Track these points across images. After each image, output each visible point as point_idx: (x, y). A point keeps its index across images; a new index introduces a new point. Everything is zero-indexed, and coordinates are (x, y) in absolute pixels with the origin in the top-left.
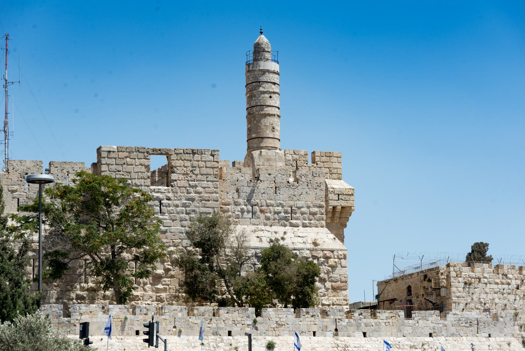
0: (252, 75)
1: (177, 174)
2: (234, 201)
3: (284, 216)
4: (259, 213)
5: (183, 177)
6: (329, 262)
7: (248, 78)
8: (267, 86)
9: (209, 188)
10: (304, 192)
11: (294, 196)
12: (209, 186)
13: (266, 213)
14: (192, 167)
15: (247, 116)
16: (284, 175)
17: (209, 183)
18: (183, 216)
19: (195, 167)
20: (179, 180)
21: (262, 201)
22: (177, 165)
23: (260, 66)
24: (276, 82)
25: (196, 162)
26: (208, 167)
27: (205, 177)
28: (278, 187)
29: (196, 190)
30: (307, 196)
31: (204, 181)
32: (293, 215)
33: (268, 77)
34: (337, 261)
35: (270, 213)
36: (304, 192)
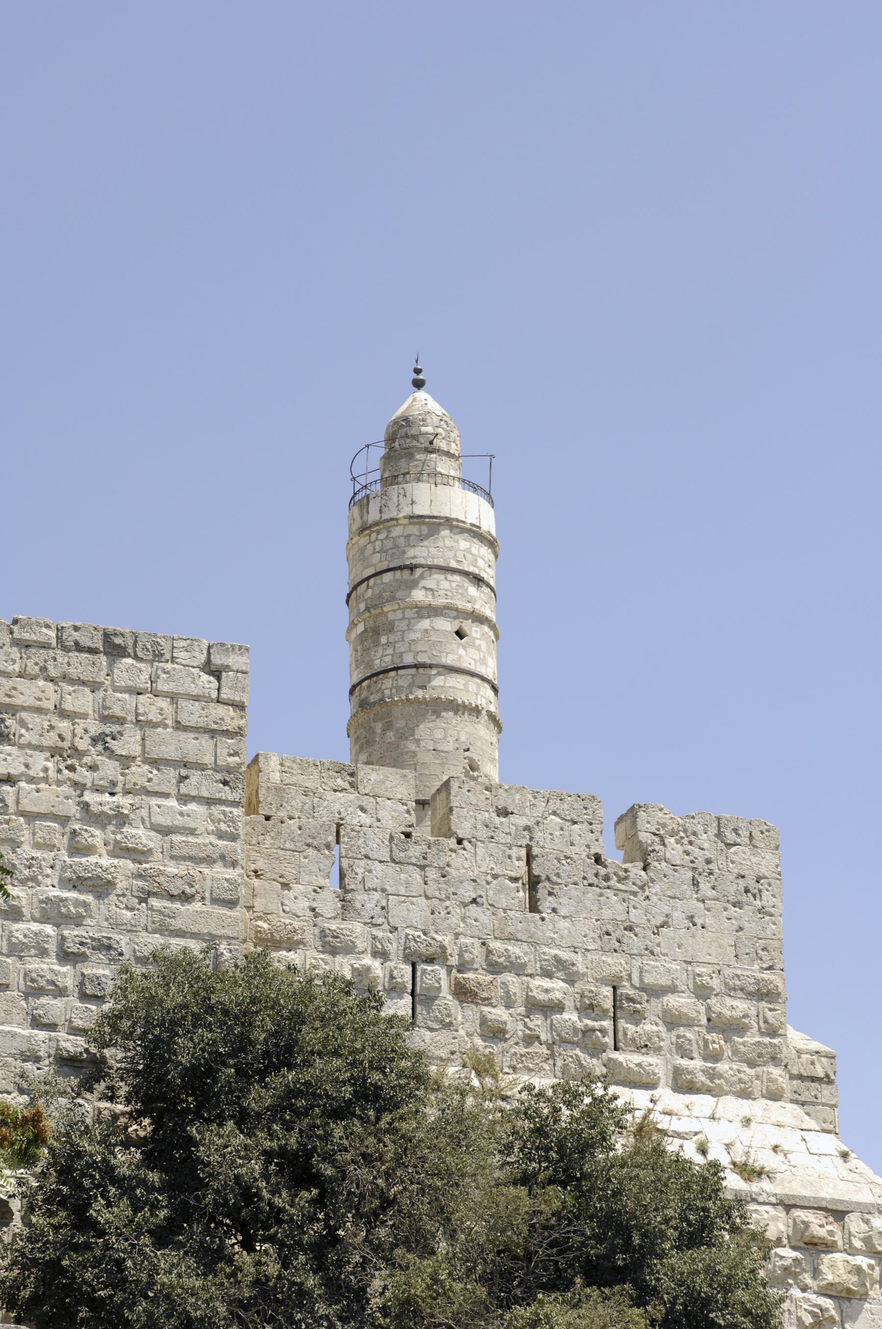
0: (378, 543)
1: (21, 747)
2: (317, 931)
3: (579, 1025)
4: (447, 998)
5: (50, 765)
6: (824, 1268)
7: (357, 556)
8: (445, 585)
9: (192, 832)
10: (678, 916)
11: (630, 929)
12: (192, 825)
13: (487, 1002)
14: (105, 719)
15: (354, 716)
16: (575, 823)
17: (192, 807)
18: (44, 966)
19: (121, 721)
20: (32, 780)
21: (463, 940)
22: (19, 700)
23: (413, 503)
24: (484, 575)
25: (126, 696)
26: (186, 729)
27: (172, 774)
28: (548, 879)
29: (119, 837)
30: (693, 936)
31: (166, 796)
32: (622, 1023)
33: (450, 549)
34: (865, 1267)
35: (508, 1007)
36: (678, 916)
